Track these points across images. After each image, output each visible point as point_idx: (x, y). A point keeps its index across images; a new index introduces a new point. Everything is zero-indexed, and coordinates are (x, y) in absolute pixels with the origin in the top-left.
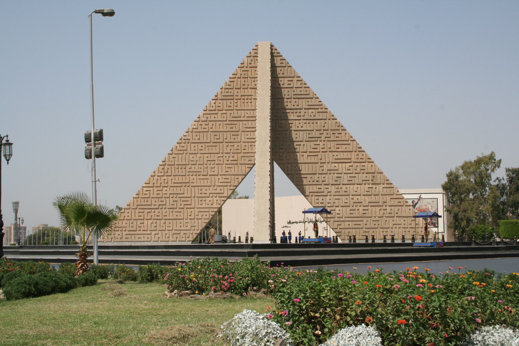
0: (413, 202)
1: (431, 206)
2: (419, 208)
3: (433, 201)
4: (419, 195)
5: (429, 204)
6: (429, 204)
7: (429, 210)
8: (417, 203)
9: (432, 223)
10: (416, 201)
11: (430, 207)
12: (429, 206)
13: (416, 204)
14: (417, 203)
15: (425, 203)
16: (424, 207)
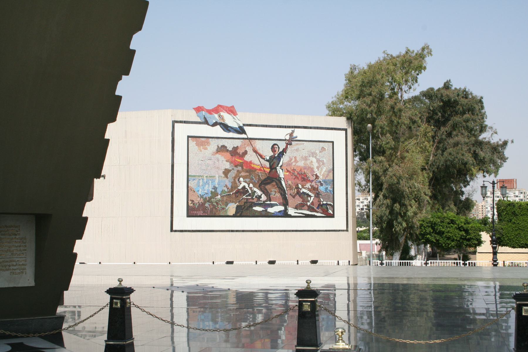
0: (273, 148)
1: (318, 161)
2: (289, 164)
3: (323, 149)
4: (290, 130)
5: (314, 154)
6: (314, 154)
7: (312, 170)
8: (284, 151)
9: (320, 206)
10: (282, 145)
11: (315, 165)
12: (314, 160)
13: (282, 154)
14: (284, 151)
15: (305, 153)
16: (301, 164)
